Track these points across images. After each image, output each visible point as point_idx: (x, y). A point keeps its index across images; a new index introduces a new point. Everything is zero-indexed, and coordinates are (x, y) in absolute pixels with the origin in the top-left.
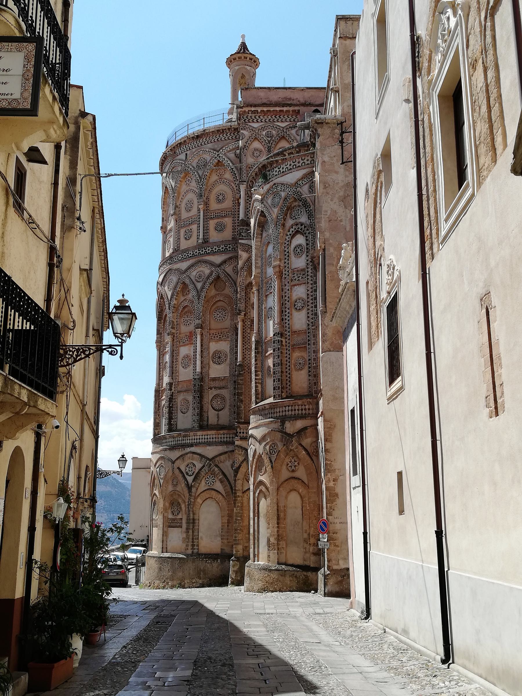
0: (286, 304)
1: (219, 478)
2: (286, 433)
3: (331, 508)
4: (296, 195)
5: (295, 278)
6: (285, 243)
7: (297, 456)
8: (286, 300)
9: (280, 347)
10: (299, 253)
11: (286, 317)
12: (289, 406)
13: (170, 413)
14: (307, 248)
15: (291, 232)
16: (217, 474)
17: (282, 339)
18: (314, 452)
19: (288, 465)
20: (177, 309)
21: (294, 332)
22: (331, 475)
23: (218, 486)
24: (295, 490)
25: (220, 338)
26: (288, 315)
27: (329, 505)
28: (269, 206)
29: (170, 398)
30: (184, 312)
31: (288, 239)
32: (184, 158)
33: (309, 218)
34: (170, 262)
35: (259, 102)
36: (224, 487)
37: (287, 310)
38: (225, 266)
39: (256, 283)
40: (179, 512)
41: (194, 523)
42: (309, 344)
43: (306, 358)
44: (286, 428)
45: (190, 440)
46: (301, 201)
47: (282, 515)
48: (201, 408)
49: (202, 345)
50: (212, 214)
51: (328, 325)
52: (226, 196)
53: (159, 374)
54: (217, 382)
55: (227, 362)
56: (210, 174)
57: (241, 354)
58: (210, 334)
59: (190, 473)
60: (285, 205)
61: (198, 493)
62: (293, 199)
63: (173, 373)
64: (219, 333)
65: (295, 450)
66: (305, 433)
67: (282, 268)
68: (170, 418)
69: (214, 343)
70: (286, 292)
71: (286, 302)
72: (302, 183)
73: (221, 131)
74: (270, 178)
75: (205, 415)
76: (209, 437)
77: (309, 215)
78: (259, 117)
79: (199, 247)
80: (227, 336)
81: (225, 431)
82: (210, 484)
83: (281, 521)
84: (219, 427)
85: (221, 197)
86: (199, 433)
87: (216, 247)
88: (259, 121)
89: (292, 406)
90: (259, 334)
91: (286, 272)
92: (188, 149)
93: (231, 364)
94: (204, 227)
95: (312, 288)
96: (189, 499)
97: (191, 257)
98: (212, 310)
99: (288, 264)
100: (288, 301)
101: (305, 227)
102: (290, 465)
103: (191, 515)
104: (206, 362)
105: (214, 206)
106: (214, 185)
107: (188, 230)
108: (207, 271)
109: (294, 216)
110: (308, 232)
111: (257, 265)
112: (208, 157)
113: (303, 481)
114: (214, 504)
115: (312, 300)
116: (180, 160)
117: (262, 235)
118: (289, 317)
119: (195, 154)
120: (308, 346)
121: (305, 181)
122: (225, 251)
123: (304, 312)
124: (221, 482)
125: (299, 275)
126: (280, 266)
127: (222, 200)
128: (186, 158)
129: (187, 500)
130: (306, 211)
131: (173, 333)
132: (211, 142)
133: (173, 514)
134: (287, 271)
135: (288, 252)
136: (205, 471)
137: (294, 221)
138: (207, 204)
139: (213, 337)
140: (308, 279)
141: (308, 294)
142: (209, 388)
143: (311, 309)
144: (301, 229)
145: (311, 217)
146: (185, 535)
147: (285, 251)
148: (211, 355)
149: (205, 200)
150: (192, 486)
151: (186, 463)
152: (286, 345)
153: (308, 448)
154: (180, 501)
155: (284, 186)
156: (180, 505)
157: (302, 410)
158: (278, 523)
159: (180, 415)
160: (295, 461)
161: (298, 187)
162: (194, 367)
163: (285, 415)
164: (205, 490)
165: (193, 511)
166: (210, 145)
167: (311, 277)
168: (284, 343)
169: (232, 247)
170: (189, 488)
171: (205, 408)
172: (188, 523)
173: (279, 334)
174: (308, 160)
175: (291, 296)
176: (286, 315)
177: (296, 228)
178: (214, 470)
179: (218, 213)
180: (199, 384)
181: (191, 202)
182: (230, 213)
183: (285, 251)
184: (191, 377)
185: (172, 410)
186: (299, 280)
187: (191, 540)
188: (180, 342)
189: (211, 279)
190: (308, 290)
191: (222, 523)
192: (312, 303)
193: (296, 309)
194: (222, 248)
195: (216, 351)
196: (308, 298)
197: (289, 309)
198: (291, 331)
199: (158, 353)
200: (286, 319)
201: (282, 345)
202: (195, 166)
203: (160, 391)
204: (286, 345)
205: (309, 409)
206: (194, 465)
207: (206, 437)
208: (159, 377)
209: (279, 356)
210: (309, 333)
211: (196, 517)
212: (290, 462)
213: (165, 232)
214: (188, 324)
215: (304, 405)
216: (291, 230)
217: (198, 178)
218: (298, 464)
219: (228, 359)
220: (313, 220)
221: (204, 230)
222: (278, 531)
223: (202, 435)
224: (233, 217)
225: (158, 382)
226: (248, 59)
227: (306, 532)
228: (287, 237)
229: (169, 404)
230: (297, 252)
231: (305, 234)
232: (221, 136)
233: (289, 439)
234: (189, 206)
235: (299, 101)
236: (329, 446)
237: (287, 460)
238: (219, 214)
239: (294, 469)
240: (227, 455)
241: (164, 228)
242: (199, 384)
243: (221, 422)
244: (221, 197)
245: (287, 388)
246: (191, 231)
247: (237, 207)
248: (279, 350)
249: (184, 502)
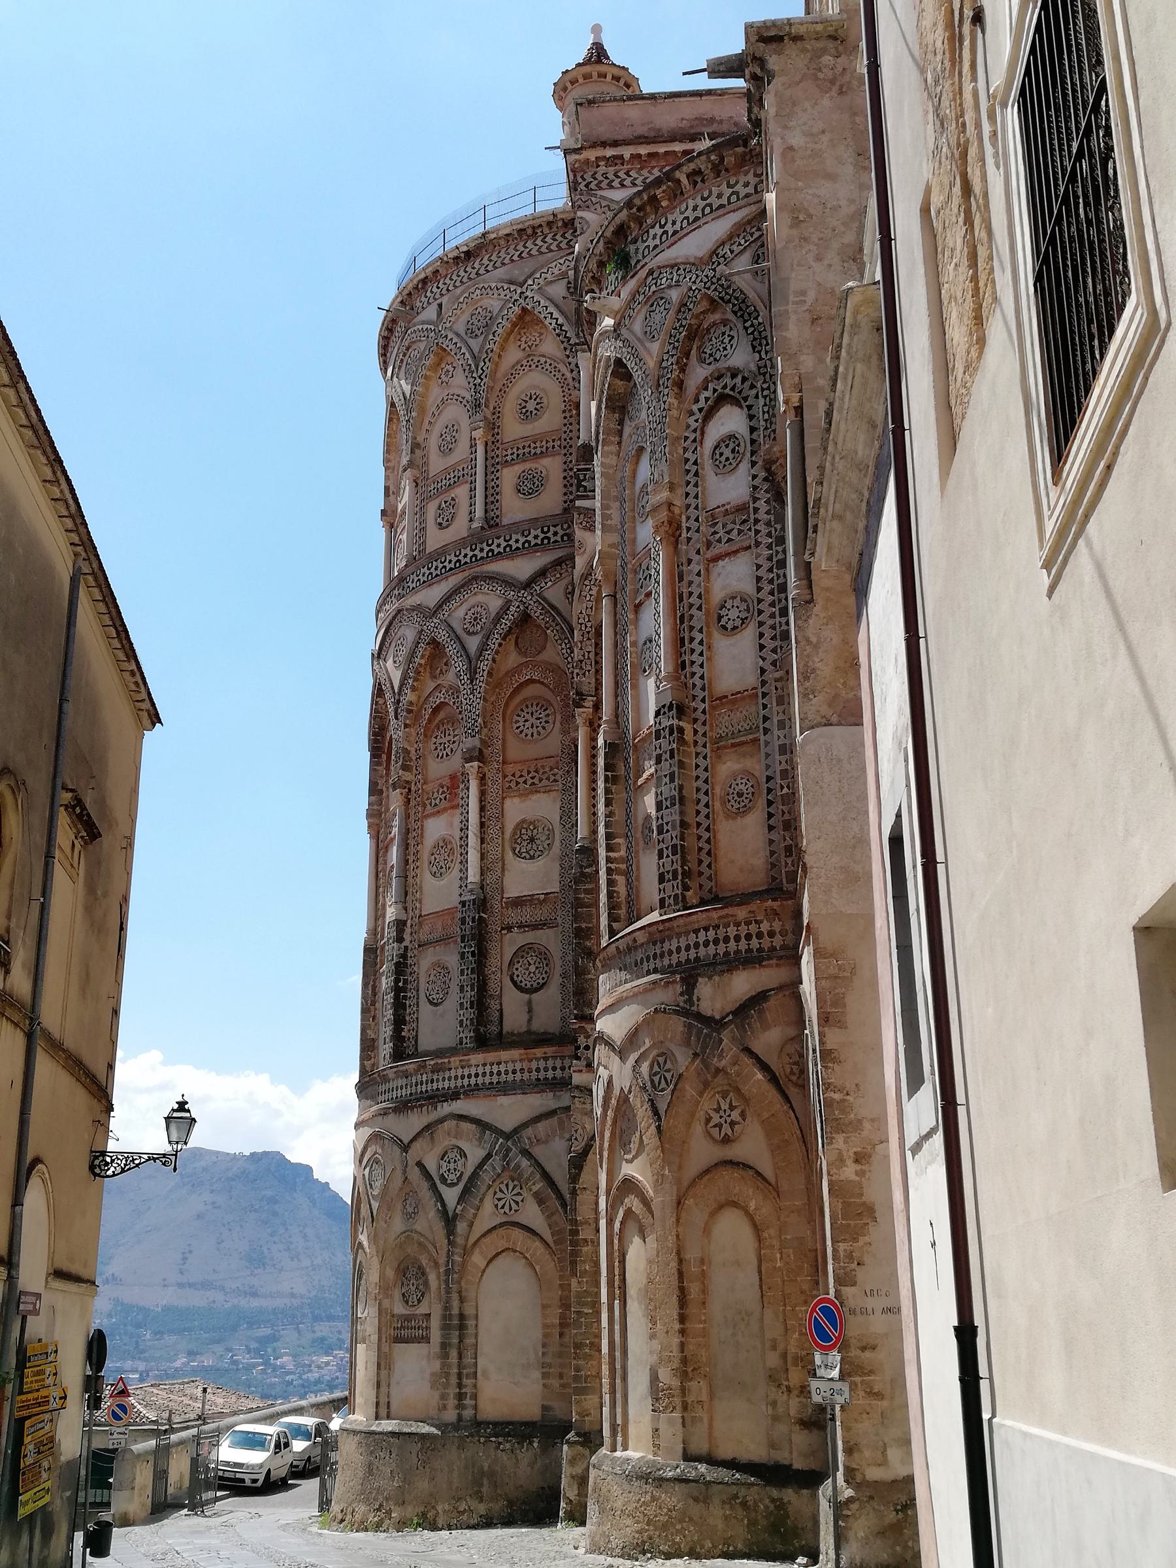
0: (692, 616)
1: (535, 1188)
2: (699, 1016)
3: (850, 1256)
4: (713, 287)
5: (717, 536)
6: (686, 438)
7: (738, 1090)
8: (691, 606)
9: (675, 746)
10: (727, 459)
11: (695, 657)
12: (706, 929)
13: (399, 1005)
14: (753, 442)
15: (702, 404)
16: (528, 1179)
17: (681, 723)
18: (792, 1073)
19: (708, 1120)
20: (418, 717)
21: (720, 699)
22: (846, 1142)
23: (532, 1214)
24: (735, 1204)
25: (533, 784)
26: (698, 649)
27: (842, 1247)
28: (638, 339)
29: (397, 965)
30: (435, 723)
31: (694, 425)
32: (434, 316)
33: (754, 347)
34: (400, 591)
35: (627, 133)
36: (549, 1217)
37: (695, 634)
39: (605, 576)
40: (423, 1295)
41: (462, 1327)
42: (766, 731)
43: (757, 774)
44: (699, 1000)
45: (450, 1079)
46: (729, 301)
47: (694, 1289)
48: (482, 986)
49: (482, 809)
50: (509, 452)
51: (819, 642)
52: (545, 400)
53: (377, 902)
56: (502, 348)
57: (586, 819)
58: (505, 776)
59: (452, 1178)
60: (681, 326)
61: (472, 1240)
62: (705, 305)
63: (406, 894)
64: (529, 772)
65: (732, 1071)
66: (761, 1012)
67: (677, 511)
68: (399, 1022)
69: (516, 800)
70: (690, 583)
71: (694, 611)
72: (732, 252)
73: (530, 231)
74: (638, 261)
75: (494, 1005)
76: (502, 1068)
77: (755, 339)
78: (627, 174)
79: (474, 539)
80: (552, 778)
81: (550, 1050)
82: (507, 1209)
83: (692, 1310)
84: (532, 1040)
85: (531, 406)
86: (477, 1058)
87: (519, 536)
88: (627, 182)
89: (717, 927)
90: (617, 723)
91: (692, 522)
92: (444, 292)
94: (486, 488)
95: (770, 559)
96: (448, 1256)
97: (451, 569)
98: (509, 712)
99: (696, 497)
100: (700, 608)
101: (744, 379)
102: (716, 1119)
103: (455, 1303)
104: (494, 852)
105: (513, 429)
106: (512, 375)
107: (446, 502)
108: (494, 603)
109: (711, 355)
110: (754, 392)
111: (609, 522)
112: (494, 304)
113: (758, 1173)
114: (520, 1266)
115: (772, 593)
116: (423, 323)
117: (620, 433)
118: (701, 654)
119: (461, 300)
120: (762, 738)
121: (740, 244)
122: (542, 543)
123: (748, 636)
124: (540, 1200)
125: (729, 527)
126: (670, 505)
127: (535, 412)
128: (440, 313)
129: (442, 1260)
130: (746, 329)
131: (407, 782)
132: (503, 264)
133: (407, 1302)
134: (693, 517)
135: (695, 463)
136: (494, 1168)
137: (712, 368)
138: (493, 427)
139: (513, 785)
140: (757, 532)
141: (759, 579)
142: (503, 929)
143: (770, 622)
144: (733, 389)
145: (760, 345)
146: (437, 1365)
147: (687, 460)
148: (508, 835)
149: (489, 416)
150: (455, 1216)
151: (438, 1150)
152: (696, 743)
153: (775, 1065)
154: (424, 1262)
155: (679, 269)
156: (423, 1274)
157: (748, 937)
158: (682, 1319)
159: (425, 1009)
160: (732, 1108)
161: (719, 264)
162: (461, 871)
163: (697, 959)
164: (494, 1228)
165: (460, 1292)
166: (500, 272)
167: (768, 524)
168: (689, 736)
169: (561, 533)
170: (449, 1221)
171: (493, 985)
172: (446, 1327)
173: (670, 708)
174: (746, 185)
175: (707, 591)
176: (693, 651)
177: (719, 388)
178: (518, 1166)
179: (524, 448)
180: (474, 918)
181: (452, 429)
182: (557, 443)
183: (687, 460)
184: (455, 901)
185: (405, 997)
186: (729, 540)
187: (454, 1380)
188: (424, 806)
189: (506, 623)
190: (759, 567)
191: (545, 1326)
192: (772, 605)
193: (724, 628)
194: (536, 537)
195: (523, 821)
196: (759, 589)
197: (701, 631)
198: (711, 696)
199: (374, 845)
200: (693, 663)
201: (682, 741)
202: (462, 332)
203: (377, 948)
204: (696, 743)
205: (771, 934)
206: (463, 1154)
207: (495, 1069)
208: (376, 910)
209: (672, 777)
210: (764, 695)
211: (469, 1310)
212: (718, 1110)
213: (392, 526)
214: (447, 755)
215: (757, 922)
216: (702, 397)
217: (470, 362)
218: (743, 1115)
219: (557, 843)
220: (767, 352)
221: (486, 497)
222: (682, 1345)
223: (484, 1065)
224: (565, 455)
225: (373, 925)
226: (609, 77)
227: (774, 1348)
228: (691, 420)
229: (397, 981)
230: (723, 459)
231: (746, 399)
232: (529, 244)
233: (708, 1036)
234: (448, 438)
235: (736, 124)
236: (834, 1038)
237: (707, 1104)
238: (527, 450)
239: (729, 1132)
240: (554, 1120)
241: (389, 512)
242: (474, 918)
243: (537, 1026)
244: (531, 406)
245: (701, 874)
246: (453, 503)
248: (672, 757)
249: (436, 1264)
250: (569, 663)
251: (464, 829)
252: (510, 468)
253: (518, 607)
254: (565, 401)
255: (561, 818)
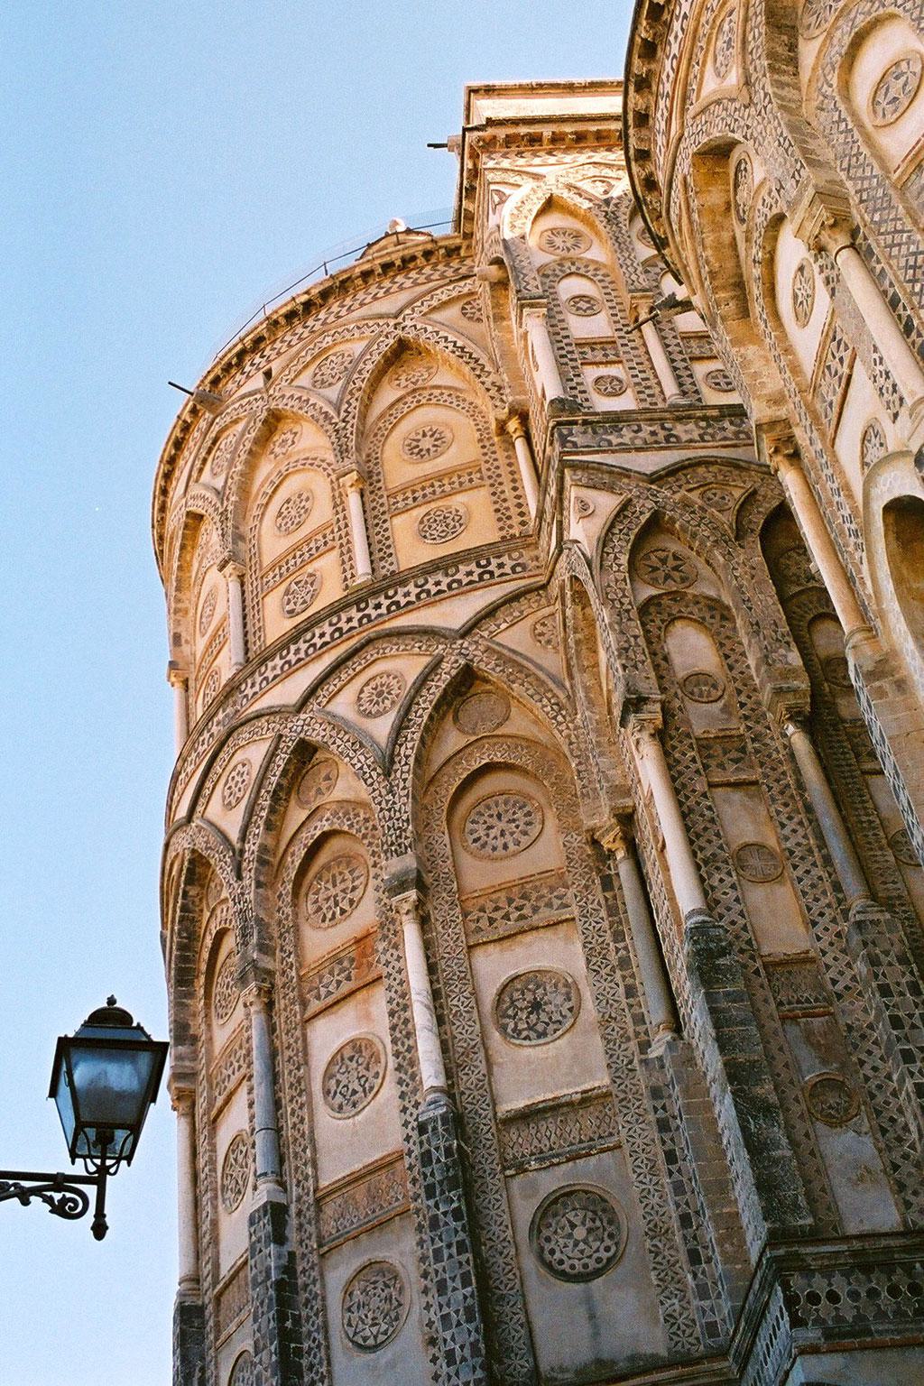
29: (279, 1285)
38: (493, 628)
49: (432, 969)
54: (549, 1127)
55: (583, 1016)
58: (465, 915)
80: (556, 902)
93: (606, 1021)
104: (464, 1032)
162: (400, 1082)
219: (589, 1004)
224: (492, 485)
229: (281, 1317)
244: (426, 443)
247: (501, 455)
250: (559, 724)
251: (399, 1009)
252: (405, 516)
253: (456, 661)
254: (479, 430)
255: (588, 961)
